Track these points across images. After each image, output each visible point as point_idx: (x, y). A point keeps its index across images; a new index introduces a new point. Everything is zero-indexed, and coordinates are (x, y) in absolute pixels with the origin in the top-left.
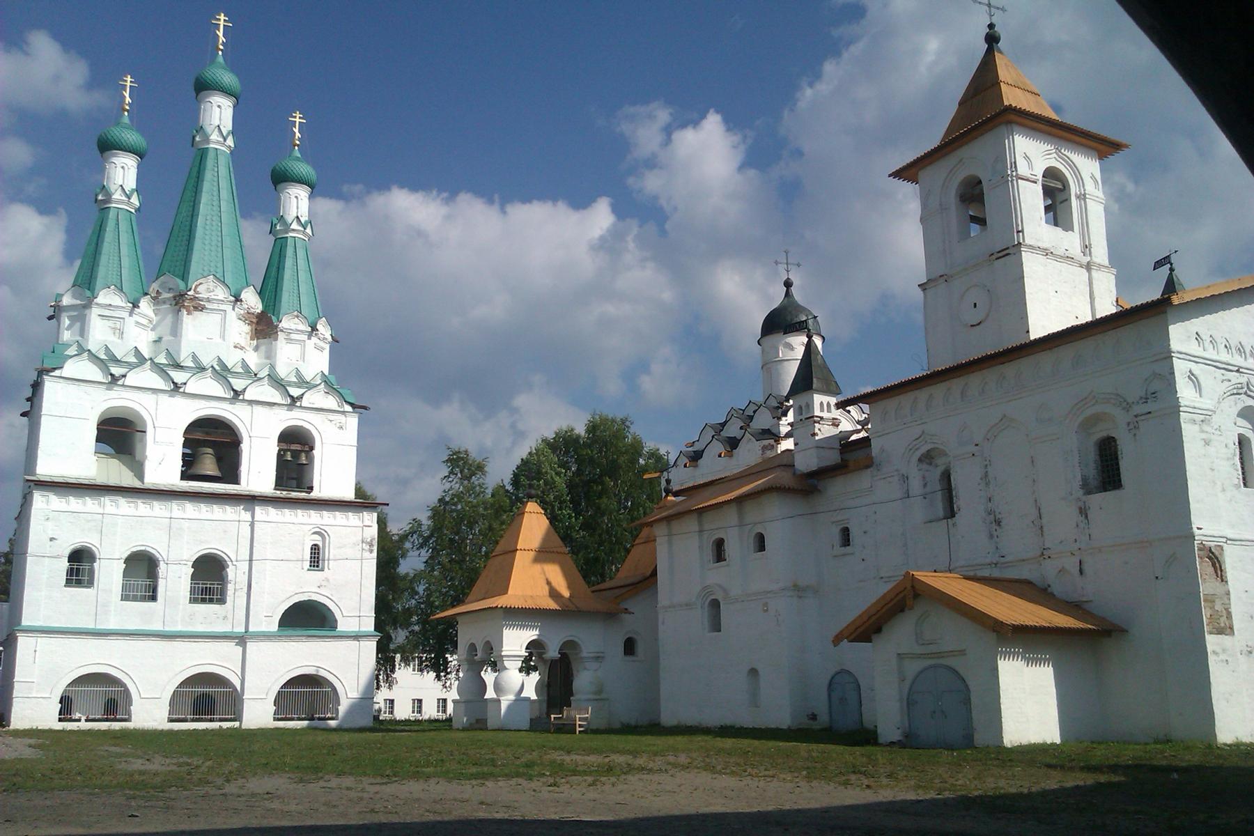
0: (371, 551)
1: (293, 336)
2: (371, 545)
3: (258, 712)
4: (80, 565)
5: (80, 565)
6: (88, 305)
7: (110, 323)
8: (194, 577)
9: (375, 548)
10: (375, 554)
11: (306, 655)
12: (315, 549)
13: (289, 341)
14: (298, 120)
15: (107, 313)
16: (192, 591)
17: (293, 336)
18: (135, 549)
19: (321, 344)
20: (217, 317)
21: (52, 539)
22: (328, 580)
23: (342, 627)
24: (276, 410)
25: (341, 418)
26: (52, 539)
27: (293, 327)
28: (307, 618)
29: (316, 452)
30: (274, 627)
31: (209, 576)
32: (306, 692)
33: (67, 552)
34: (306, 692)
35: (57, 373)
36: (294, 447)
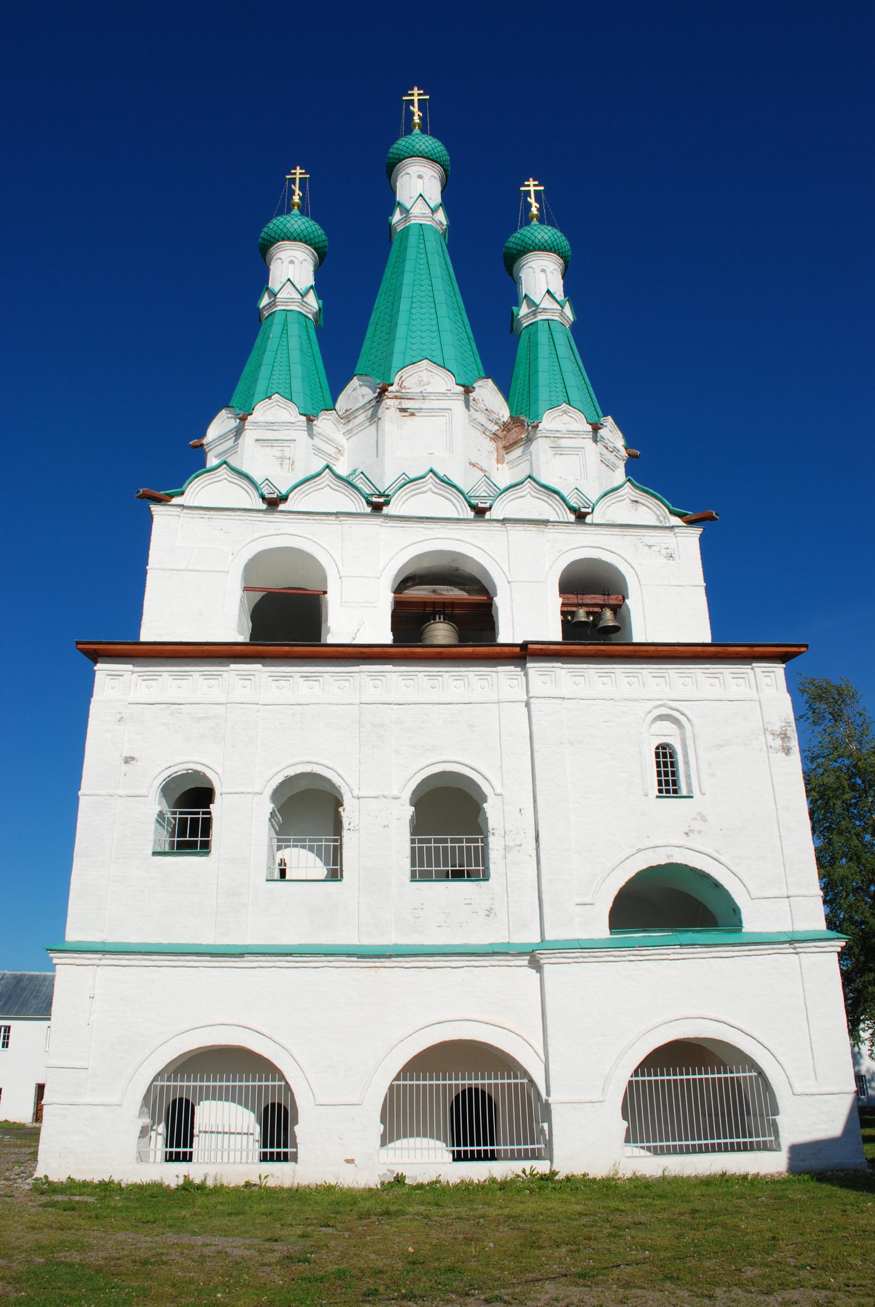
0: (787, 751)
1: (564, 442)
2: (785, 737)
3: (589, 1137)
4: (190, 815)
5: (190, 815)
6: (239, 432)
7: (276, 452)
8: (419, 826)
9: (794, 744)
10: (796, 757)
11: (684, 990)
12: (665, 757)
13: (557, 450)
14: (532, 189)
15: (269, 435)
16: (417, 856)
17: (564, 442)
18: (292, 772)
19: (611, 457)
20: (439, 422)
21: (128, 760)
22: (704, 819)
23: (751, 924)
24: (550, 533)
25: (667, 538)
26: (128, 760)
27: (563, 428)
28: (670, 905)
29: (632, 603)
30: (599, 927)
31: (450, 823)
32: (693, 1084)
33: (159, 783)
34: (693, 1084)
35: (175, 501)
36: (589, 599)
